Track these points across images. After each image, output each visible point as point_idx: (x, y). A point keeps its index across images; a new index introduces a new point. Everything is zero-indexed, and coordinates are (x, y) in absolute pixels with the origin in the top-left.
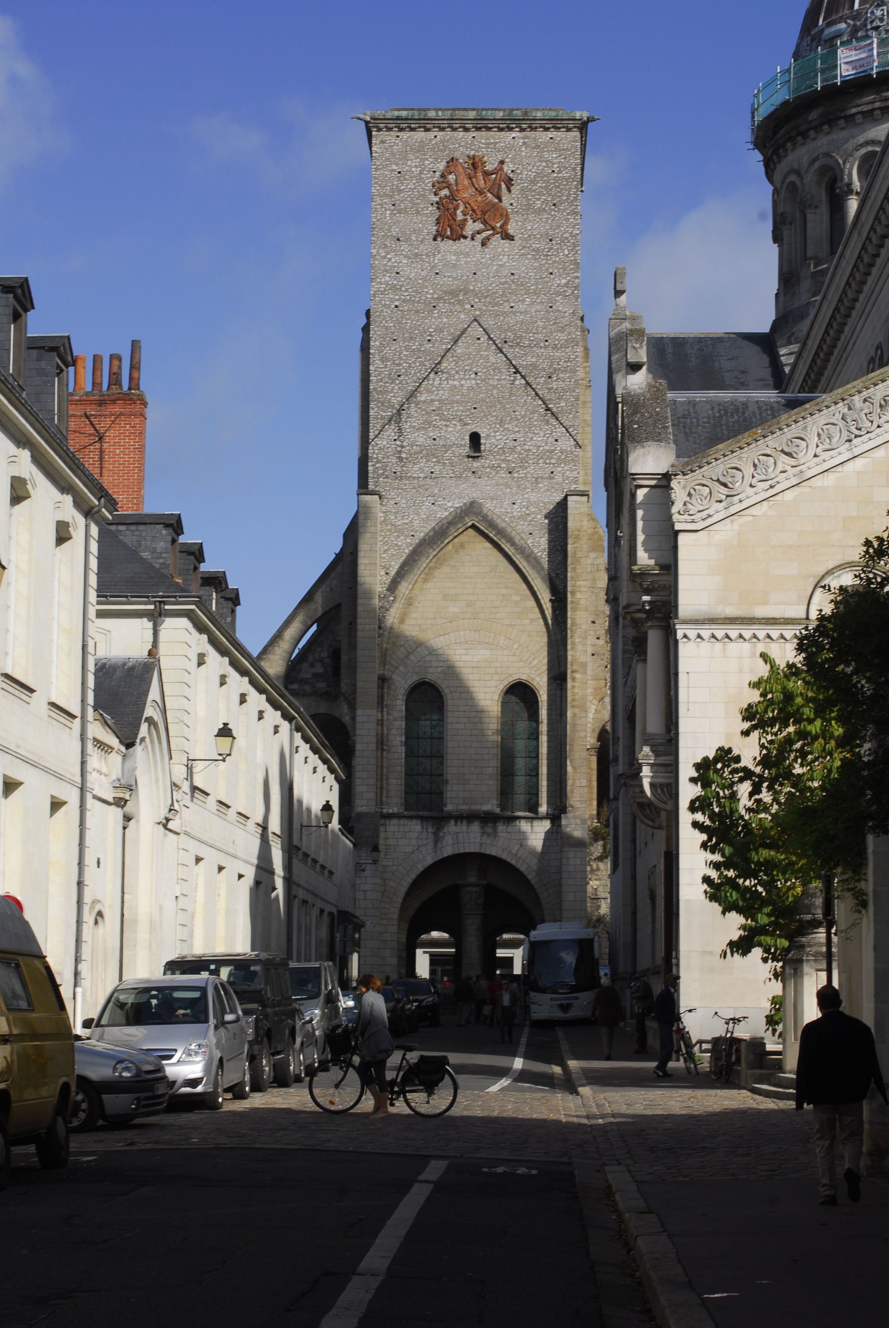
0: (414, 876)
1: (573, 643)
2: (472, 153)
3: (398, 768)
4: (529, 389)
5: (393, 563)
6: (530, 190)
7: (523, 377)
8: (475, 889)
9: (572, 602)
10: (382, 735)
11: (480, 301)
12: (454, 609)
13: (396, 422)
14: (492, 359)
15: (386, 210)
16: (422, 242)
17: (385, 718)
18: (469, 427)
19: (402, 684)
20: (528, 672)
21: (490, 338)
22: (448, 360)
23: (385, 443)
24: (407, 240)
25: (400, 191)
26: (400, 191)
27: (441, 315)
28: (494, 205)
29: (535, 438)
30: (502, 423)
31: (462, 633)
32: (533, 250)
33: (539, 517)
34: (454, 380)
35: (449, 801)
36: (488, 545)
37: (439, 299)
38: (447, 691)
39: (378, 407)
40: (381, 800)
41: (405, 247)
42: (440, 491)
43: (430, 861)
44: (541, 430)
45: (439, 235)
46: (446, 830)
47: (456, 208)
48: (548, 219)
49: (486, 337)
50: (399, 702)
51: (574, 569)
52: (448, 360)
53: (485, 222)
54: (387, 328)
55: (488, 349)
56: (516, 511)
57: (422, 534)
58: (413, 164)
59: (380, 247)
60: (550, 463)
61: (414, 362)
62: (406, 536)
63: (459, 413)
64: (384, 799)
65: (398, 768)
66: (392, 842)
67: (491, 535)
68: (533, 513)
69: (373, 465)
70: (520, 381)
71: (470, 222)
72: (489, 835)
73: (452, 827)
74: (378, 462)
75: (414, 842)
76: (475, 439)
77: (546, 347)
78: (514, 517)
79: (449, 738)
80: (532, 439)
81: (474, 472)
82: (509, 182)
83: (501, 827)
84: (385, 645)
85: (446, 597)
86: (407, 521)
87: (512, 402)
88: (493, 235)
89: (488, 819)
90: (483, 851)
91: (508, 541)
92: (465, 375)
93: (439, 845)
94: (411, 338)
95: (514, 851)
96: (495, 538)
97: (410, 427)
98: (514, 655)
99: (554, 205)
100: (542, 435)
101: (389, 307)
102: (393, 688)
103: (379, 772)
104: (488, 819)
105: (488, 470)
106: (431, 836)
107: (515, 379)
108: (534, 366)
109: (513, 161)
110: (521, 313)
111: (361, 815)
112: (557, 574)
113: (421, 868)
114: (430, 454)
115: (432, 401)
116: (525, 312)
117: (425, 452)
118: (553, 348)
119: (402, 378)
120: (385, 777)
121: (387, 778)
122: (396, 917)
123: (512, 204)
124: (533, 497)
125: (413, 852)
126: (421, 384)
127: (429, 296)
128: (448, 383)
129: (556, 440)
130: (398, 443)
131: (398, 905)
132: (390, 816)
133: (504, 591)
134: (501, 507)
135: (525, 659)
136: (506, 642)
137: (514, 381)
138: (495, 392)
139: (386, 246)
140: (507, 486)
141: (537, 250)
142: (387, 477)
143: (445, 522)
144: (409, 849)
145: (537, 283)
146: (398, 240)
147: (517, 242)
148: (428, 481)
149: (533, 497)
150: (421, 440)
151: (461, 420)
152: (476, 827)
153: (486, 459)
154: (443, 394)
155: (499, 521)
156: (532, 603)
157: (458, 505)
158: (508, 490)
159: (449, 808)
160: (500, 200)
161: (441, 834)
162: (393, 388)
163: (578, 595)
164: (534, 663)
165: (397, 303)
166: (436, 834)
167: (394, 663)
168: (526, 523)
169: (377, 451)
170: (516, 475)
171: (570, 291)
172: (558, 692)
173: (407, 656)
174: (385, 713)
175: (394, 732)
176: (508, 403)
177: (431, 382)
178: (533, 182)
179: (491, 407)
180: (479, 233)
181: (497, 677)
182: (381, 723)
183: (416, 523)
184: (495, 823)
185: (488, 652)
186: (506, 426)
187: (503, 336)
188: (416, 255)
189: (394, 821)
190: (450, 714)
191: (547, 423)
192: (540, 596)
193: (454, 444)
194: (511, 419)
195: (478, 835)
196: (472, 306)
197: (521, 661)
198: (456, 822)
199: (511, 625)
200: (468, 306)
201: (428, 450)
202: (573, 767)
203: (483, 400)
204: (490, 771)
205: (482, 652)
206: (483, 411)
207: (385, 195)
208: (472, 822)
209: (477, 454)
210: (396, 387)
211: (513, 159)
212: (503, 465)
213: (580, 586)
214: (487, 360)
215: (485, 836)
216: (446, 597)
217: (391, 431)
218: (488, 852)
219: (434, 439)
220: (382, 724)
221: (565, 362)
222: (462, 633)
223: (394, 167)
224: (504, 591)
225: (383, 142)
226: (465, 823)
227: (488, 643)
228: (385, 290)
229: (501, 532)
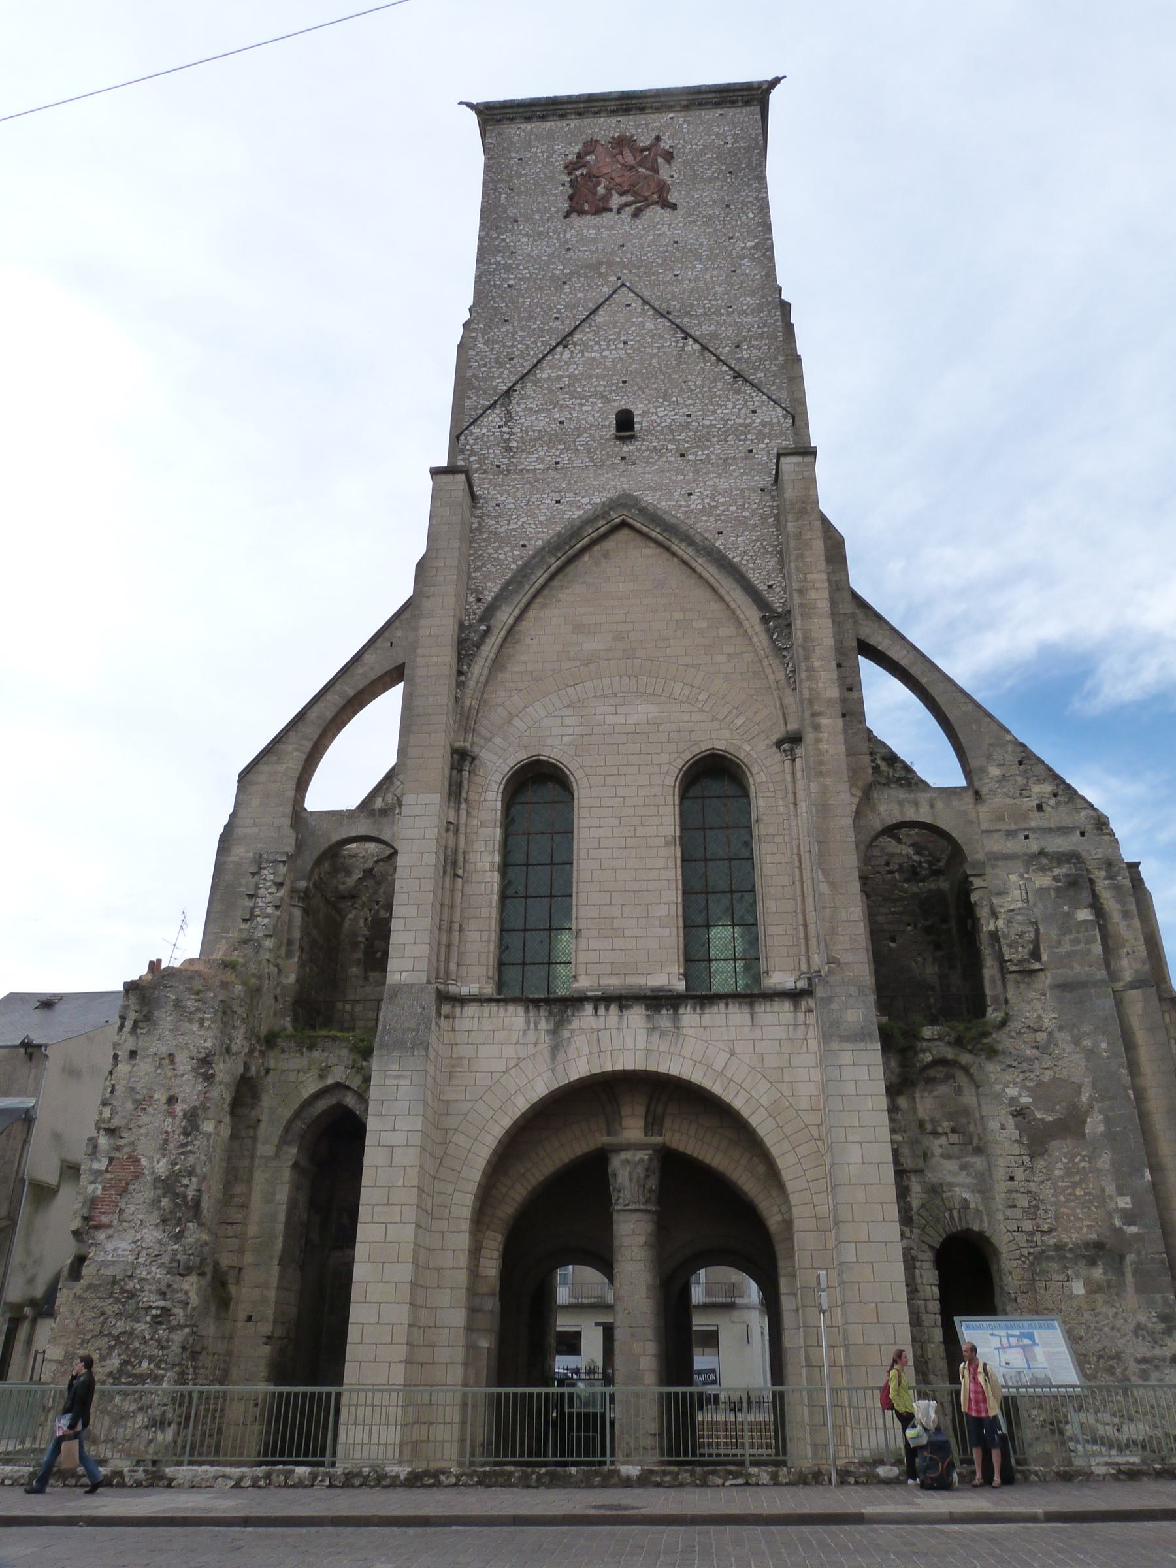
0: (507, 1122)
1: (810, 669)
2: (617, 135)
3: (485, 912)
4: (707, 354)
5: (489, 584)
6: (698, 162)
7: (696, 341)
9: (801, 605)
10: (456, 852)
11: (630, 272)
12: (590, 645)
13: (502, 405)
14: (650, 325)
15: (500, 193)
16: (548, 220)
17: (463, 820)
18: (616, 404)
19: (496, 765)
20: (728, 736)
21: (645, 302)
22: (583, 331)
23: (484, 431)
24: (528, 219)
25: (521, 175)
26: (521, 175)
27: (573, 290)
28: (646, 177)
29: (719, 411)
30: (665, 397)
31: (606, 681)
32: (705, 216)
33: (733, 508)
34: (593, 351)
35: (581, 969)
36: (651, 550)
37: (572, 274)
38: (579, 774)
39: (478, 397)
40: (447, 972)
41: (524, 227)
42: (569, 484)
43: (541, 1088)
44: (729, 400)
45: (575, 208)
46: (575, 1024)
47: (599, 184)
48: (722, 187)
49: (640, 302)
50: (491, 795)
51: (802, 556)
52: (583, 331)
53: (635, 194)
54: (495, 309)
55: (643, 313)
56: (695, 503)
57: (540, 543)
58: (540, 151)
59: (491, 229)
60: (746, 439)
61: (535, 343)
62: (513, 547)
63: (600, 389)
64: (453, 966)
65: (485, 912)
66: (464, 1051)
67: (653, 534)
68: (723, 504)
69: (463, 459)
70: (691, 346)
71: (615, 196)
72: (663, 1033)
73: (586, 1018)
74: (473, 453)
75: (509, 1051)
76: (625, 423)
77: (728, 314)
78: (692, 511)
79: (583, 854)
80: (714, 412)
81: (623, 458)
82: (669, 156)
83: (688, 1016)
84: (468, 702)
85: (578, 628)
86: (515, 526)
87: (683, 371)
88: (648, 206)
89: (658, 1001)
90: (652, 1067)
91: (682, 540)
92: (608, 345)
93: (561, 1057)
94: (530, 317)
96: (660, 538)
97: (524, 410)
98: (701, 710)
99: (730, 173)
100: (730, 406)
101: (500, 286)
102: (481, 772)
103: (445, 917)
104: (658, 1001)
105: (647, 453)
106: (546, 1038)
107: (685, 345)
108: (714, 335)
109: (671, 137)
110: (690, 281)
111: (399, 988)
112: (770, 587)
113: (522, 1104)
114: (552, 440)
115: (559, 378)
116: (697, 279)
117: (546, 438)
118: (739, 314)
119: (516, 360)
120: (456, 927)
121: (461, 930)
122: (467, 1212)
123: (672, 177)
124: (722, 483)
125: (508, 1071)
126: (543, 358)
127: (558, 272)
128: (583, 356)
129: (754, 412)
130: (505, 429)
131: (473, 1187)
132: (462, 1001)
133: (678, 616)
134: (670, 499)
135: (720, 717)
136: (686, 692)
137: (683, 347)
138: (655, 361)
139: (498, 227)
140: (677, 471)
141: (710, 217)
142: (485, 472)
143: (577, 522)
144: (500, 1066)
145: (711, 249)
146: (516, 221)
147: (681, 211)
148: (551, 473)
149: (722, 483)
150: (542, 424)
151: (603, 396)
152: (636, 1016)
153: (643, 440)
154: (575, 369)
155: (666, 517)
156: (727, 630)
157: (599, 501)
158: (680, 477)
159: (584, 983)
160: (655, 170)
161: (566, 1034)
162: (502, 373)
163: (813, 595)
164: (739, 721)
165: (511, 282)
166: (554, 1032)
167: (484, 732)
168: (712, 519)
169: (471, 442)
170: (691, 457)
171: (760, 254)
172: (787, 763)
173: (509, 722)
174: (463, 813)
175: (480, 846)
176: (676, 373)
177: (557, 357)
178: (702, 153)
179: (649, 379)
180: (627, 205)
181: (672, 747)
182: (452, 827)
183: (529, 529)
184: (676, 1008)
185: (653, 708)
186: (674, 399)
187: (665, 306)
188: (540, 233)
189: (472, 1009)
190: (584, 813)
191: (738, 391)
192: (741, 616)
193: (592, 425)
194: (682, 390)
195: (642, 1035)
196: (619, 278)
197: (714, 719)
198: (596, 1009)
199: (693, 665)
200: (614, 278)
201: (550, 436)
202: (832, 884)
203: (638, 372)
204: (663, 910)
205: (641, 708)
206: (637, 384)
207: (501, 180)
208: (629, 1007)
209: (628, 433)
210: (506, 372)
211: (671, 137)
212: (670, 447)
213: (813, 581)
214: (642, 325)
215: (657, 1033)
216: (578, 628)
217: (495, 418)
218: (662, 1069)
219: (562, 423)
220: (457, 830)
221: (759, 327)
222: (606, 681)
223: (513, 155)
224: (678, 616)
225: (500, 134)
226: (614, 1009)
227: (653, 694)
228: (495, 270)
229: (671, 529)
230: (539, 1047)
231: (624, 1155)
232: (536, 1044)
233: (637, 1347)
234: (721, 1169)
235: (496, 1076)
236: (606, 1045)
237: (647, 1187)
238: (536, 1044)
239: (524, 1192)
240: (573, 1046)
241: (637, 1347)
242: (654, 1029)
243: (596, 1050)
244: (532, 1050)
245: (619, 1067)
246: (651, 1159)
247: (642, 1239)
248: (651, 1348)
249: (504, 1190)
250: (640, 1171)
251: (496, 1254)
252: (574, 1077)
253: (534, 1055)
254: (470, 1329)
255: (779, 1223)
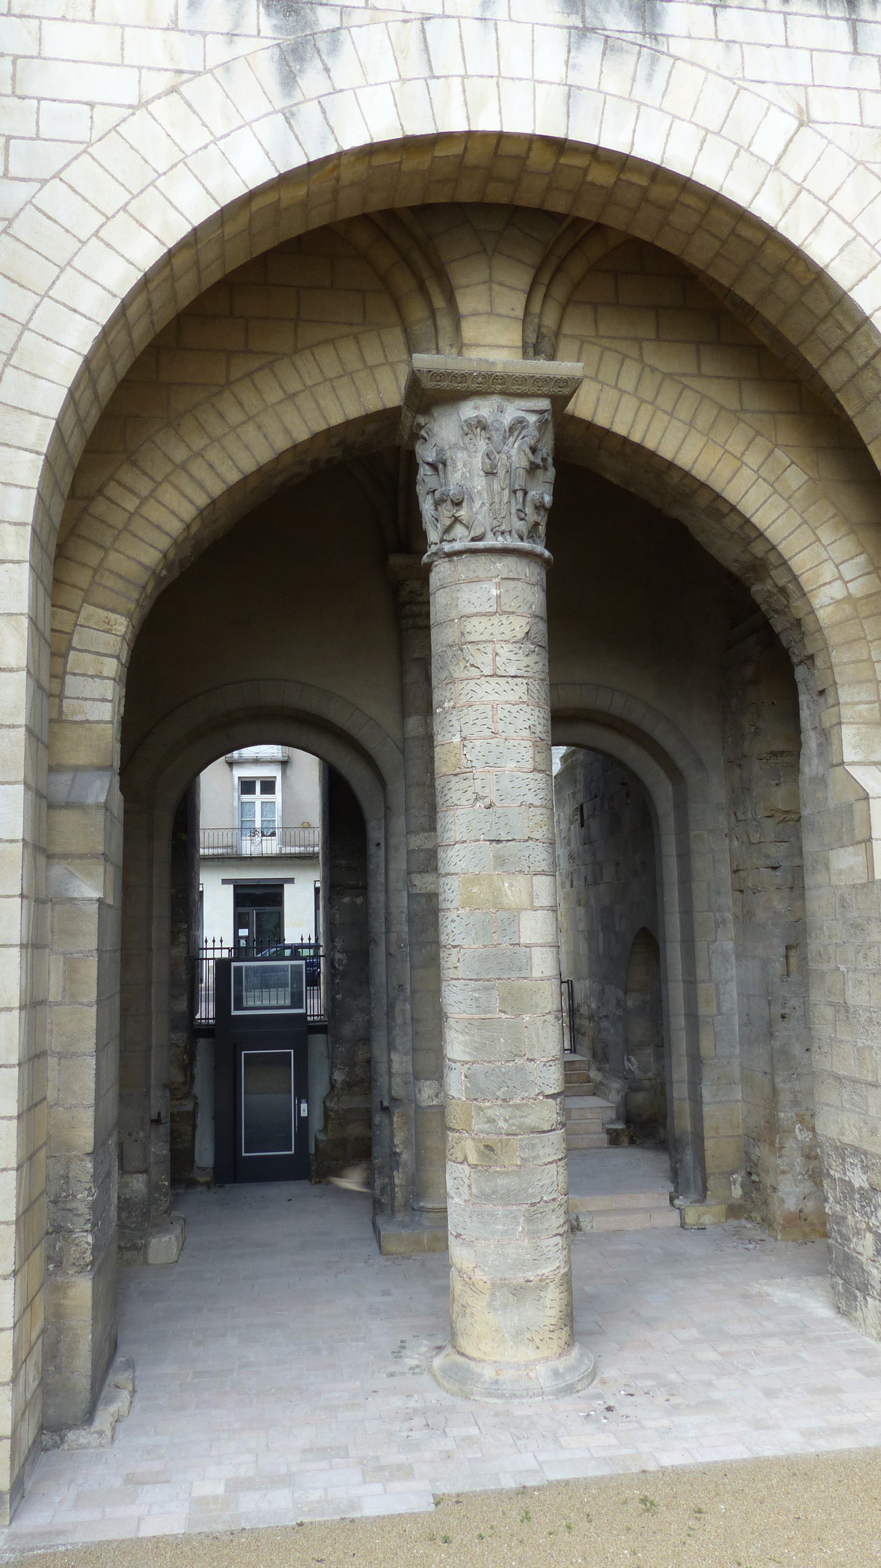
0: (147, 253)
8: (513, 410)
72: (610, 46)
90: (583, 132)
93: (311, 81)
95: (768, 147)
144: (120, 87)
195: (552, 44)
215: (594, 47)
218: (613, 140)
230: (243, 46)
231: (469, 410)
232: (231, 36)
233: (514, 891)
234: (701, 472)
235: (105, 118)
236: (447, 60)
237: (532, 493)
238: (231, 36)
239: (188, 512)
240: (347, 48)
241: (514, 891)
242: (585, 32)
243: (415, 66)
244: (218, 51)
245: (487, 123)
246: (542, 425)
247: (519, 625)
248: (544, 889)
249: (131, 504)
250: (516, 454)
251: (111, 667)
252: (354, 138)
253: (226, 66)
254: (41, 848)
255: (838, 602)
